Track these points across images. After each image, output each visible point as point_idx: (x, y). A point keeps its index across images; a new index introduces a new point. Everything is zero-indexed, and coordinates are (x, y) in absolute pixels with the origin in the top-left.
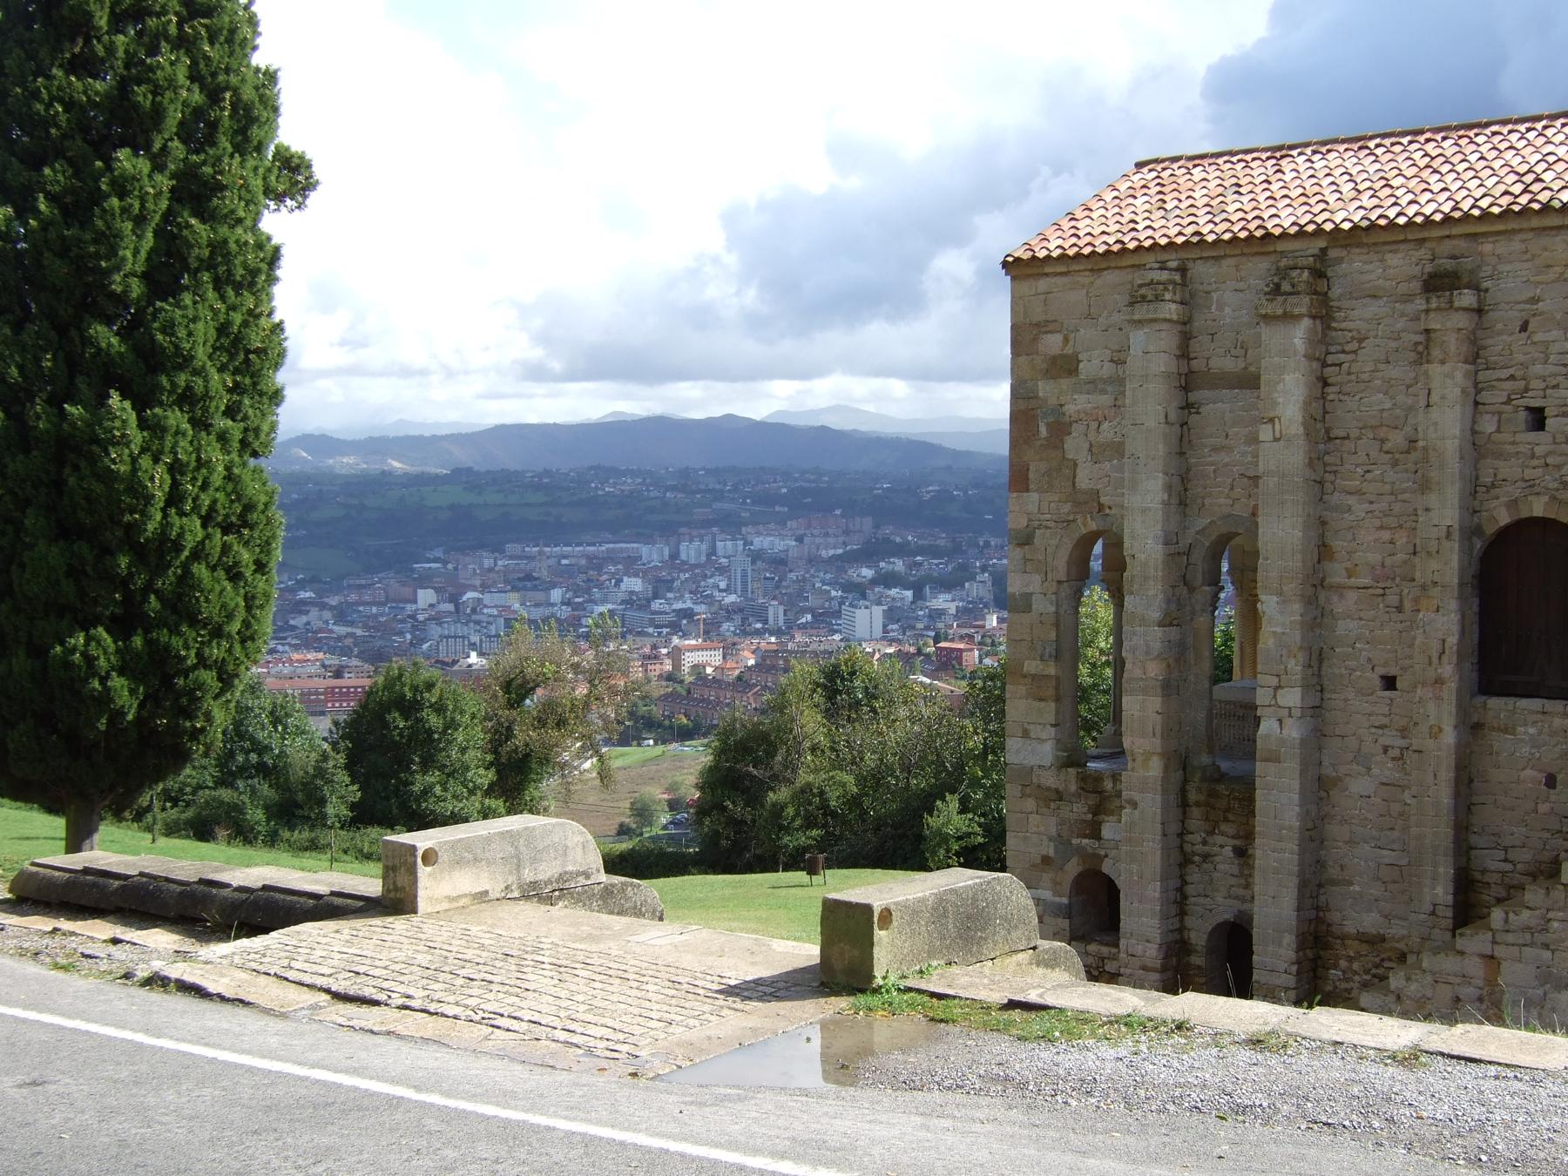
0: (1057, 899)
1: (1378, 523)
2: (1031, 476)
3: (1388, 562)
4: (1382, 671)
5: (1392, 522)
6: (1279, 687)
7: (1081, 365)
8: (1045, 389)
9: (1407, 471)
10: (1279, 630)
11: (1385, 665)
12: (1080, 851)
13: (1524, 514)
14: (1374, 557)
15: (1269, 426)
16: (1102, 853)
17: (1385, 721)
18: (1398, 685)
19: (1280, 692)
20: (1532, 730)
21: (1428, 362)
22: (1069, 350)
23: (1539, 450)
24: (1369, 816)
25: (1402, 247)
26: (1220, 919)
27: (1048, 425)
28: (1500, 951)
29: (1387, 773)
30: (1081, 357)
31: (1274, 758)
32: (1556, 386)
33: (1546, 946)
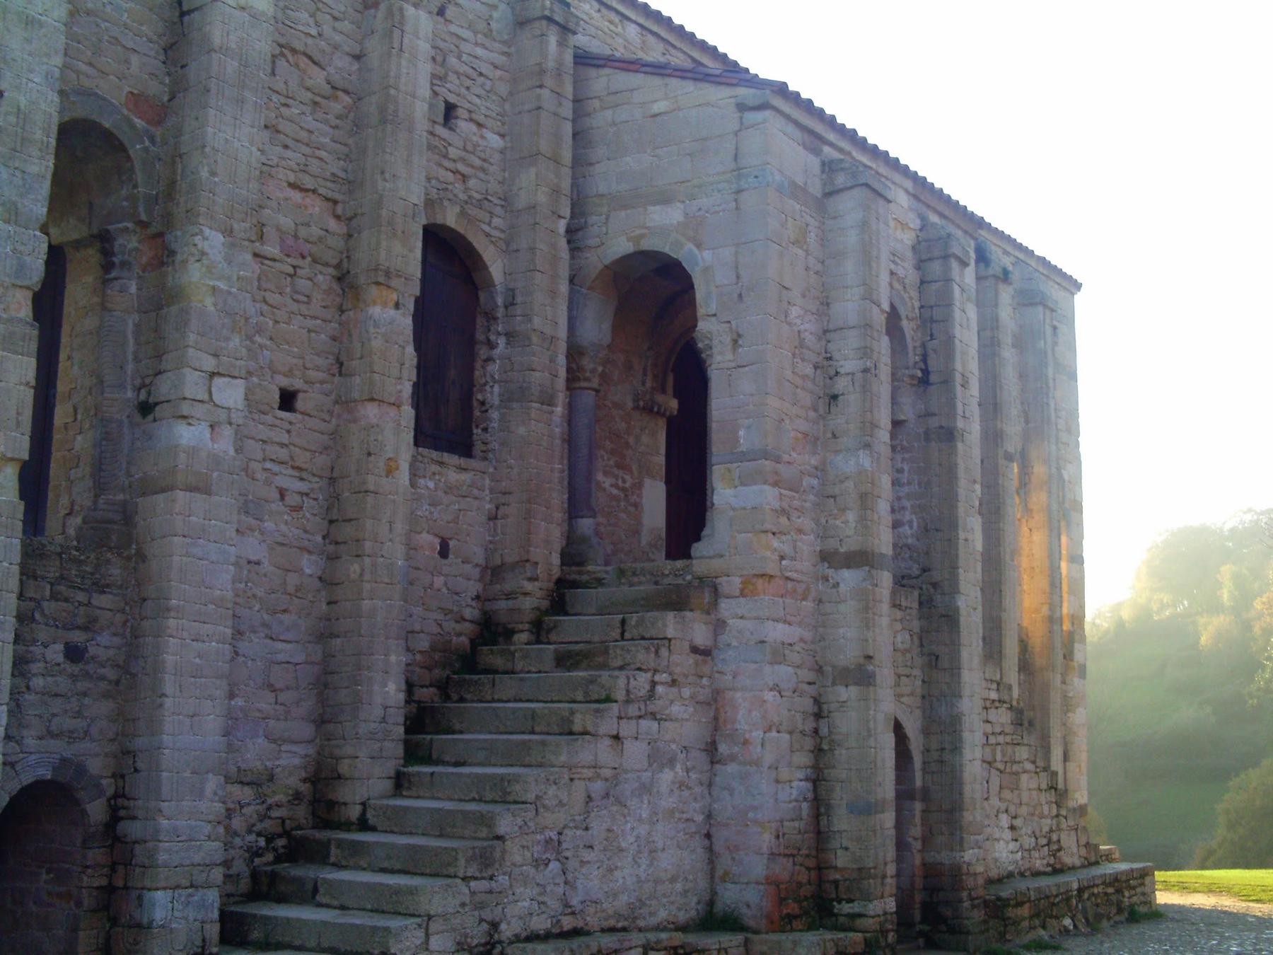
1: (292, 178)
3: (303, 232)
4: (284, 382)
5: (308, 182)
6: (213, 375)
9: (326, 122)
10: (222, 285)
11: (289, 374)
13: (439, 221)
14: (287, 222)
17: (283, 454)
18: (300, 404)
19: (218, 381)
20: (431, 485)
23: (453, 153)
24: (260, 592)
28: (627, 729)
29: (283, 528)
31: (201, 487)
32: (468, 88)
33: (653, 716)
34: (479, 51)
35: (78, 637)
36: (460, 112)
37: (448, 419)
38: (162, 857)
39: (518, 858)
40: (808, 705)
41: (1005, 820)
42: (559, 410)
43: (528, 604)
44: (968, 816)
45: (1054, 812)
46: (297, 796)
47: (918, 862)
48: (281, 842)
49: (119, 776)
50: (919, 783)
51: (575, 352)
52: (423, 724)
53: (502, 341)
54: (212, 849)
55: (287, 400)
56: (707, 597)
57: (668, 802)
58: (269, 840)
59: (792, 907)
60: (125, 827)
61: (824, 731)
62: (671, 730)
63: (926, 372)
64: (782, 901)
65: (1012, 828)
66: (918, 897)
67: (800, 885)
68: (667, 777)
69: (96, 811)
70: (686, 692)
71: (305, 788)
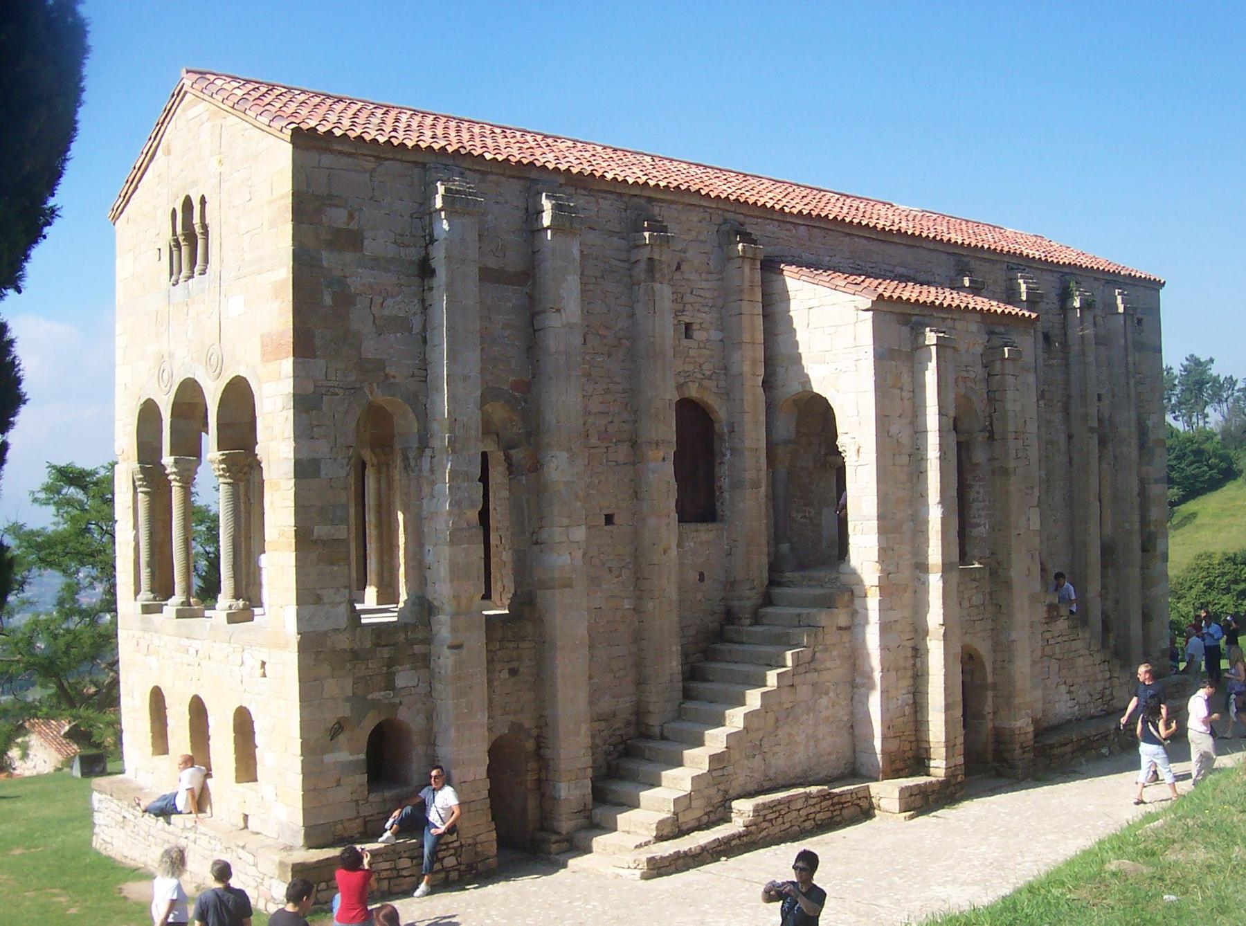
0: (355, 757)
2: (317, 342)
7: (366, 243)
8: (328, 259)
11: (608, 508)
12: (375, 704)
13: (686, 396)
15: (557, 315)
16: (397, 701)
18: (616, 519)
21: (653, 281)
22: (353, 226)
25: (609, 196)
26: (498, 734)
27: (334, 294)
30: (366, 234)
31: (568, 584)
34: (704, 285)
35: (514, 665)
36: (695, 327)
37: (699, 501)
38: (562, 766)
39: (738, 757)
40: (909, 653)
41: (1063, 689)
42: (763, 489)
43: (748, 604)
44: (1017, 701)
45: (1108, 675)
46: (628, 723)
47: (990, 725)
48: (621, 747)
49: (539, 727)
50: (990, 680)
51: (770, 446)
52: (693, 674)
53: (728, 453)
54: (588, 761)
55: (609, 519)
56: (846, 598)
57: (825, 713)
58: (615, 747)
59: (899, 765)
60: (543, 752)
61: (919, 664)
62: (825, 676)
63: (992, 433)
64: (893, 762)
65: (1069, 692)
66: (990, 747)
67: (905, 752)
68: (824, 701)
69: (530, 745)
70: (835, 653)
71: (632, 718)
